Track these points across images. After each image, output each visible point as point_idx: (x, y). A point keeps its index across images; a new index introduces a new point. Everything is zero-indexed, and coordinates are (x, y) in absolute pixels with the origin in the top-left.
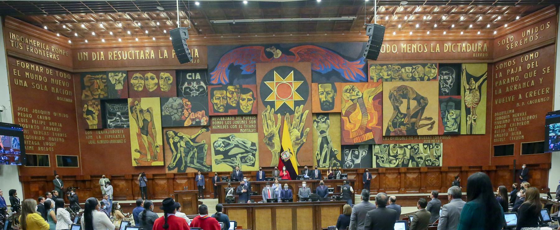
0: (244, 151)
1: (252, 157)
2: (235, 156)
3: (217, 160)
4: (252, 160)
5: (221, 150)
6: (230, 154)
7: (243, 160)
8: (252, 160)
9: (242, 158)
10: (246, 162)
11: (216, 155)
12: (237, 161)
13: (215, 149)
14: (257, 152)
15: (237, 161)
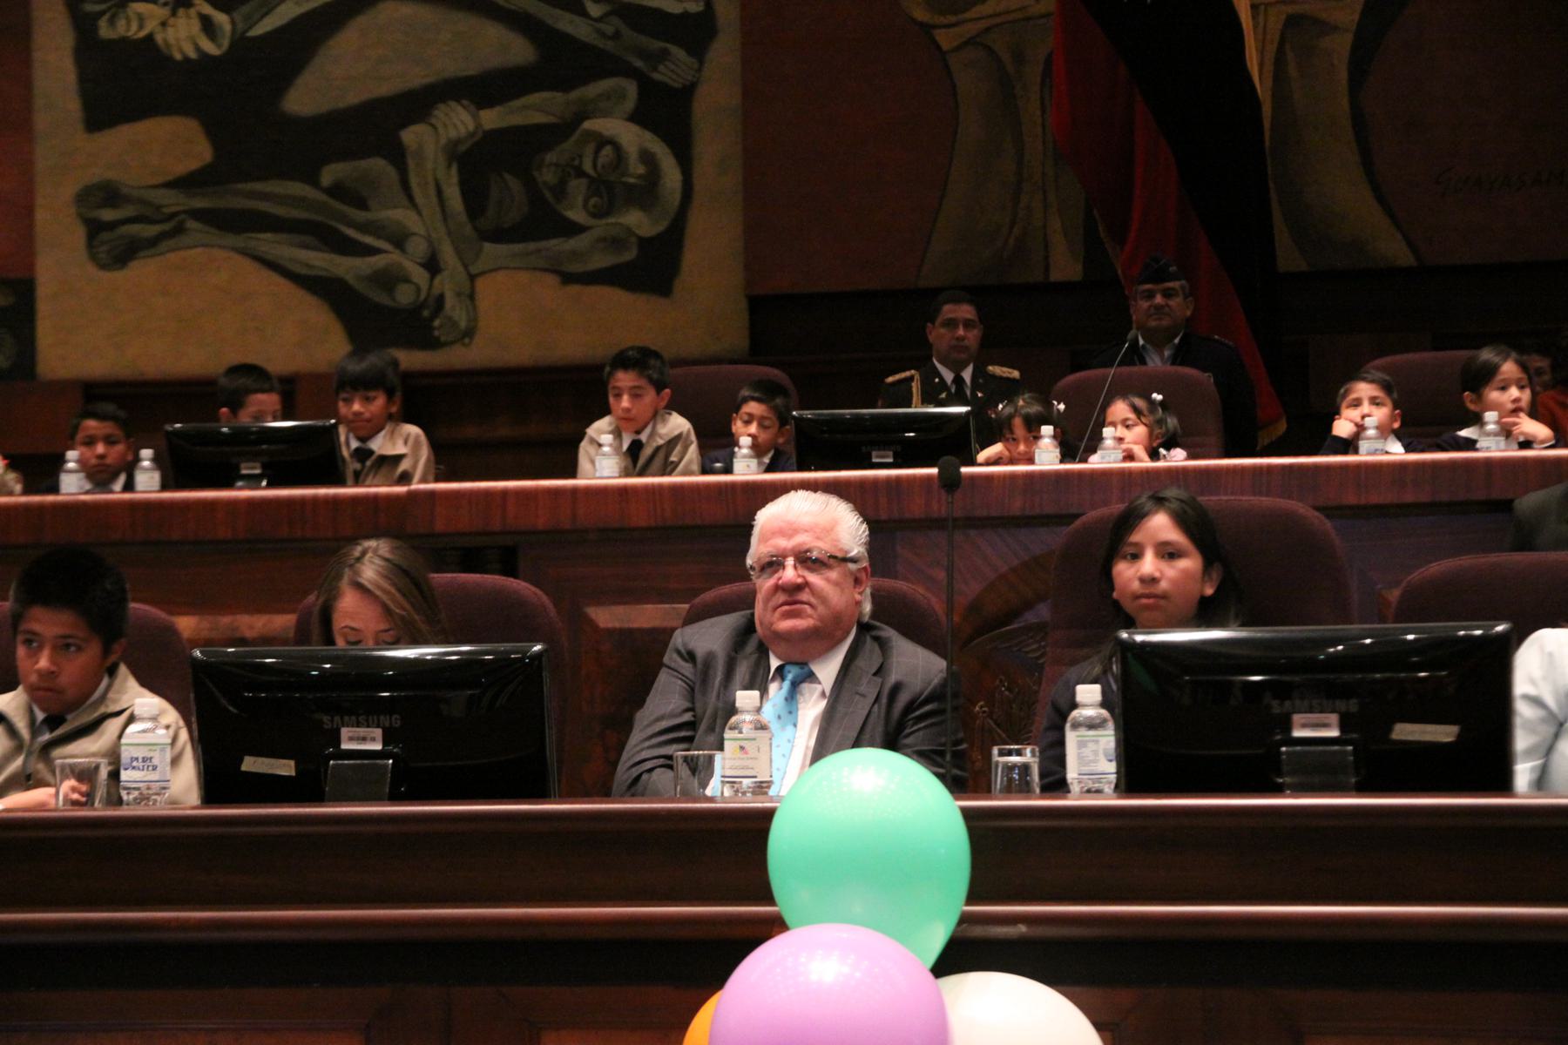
0: (517, 50)
1: (631, 137)
2: (377, 126)
3: (109, 194)
4: (646, 193)
5: (183, 37)
6: (306, 97)
7: (509, 194)
8: (646, 193)
9: (477, 163)
10: (542, 222)
11: (99, 116)
12: (415, 217)
13: (84, 26)
14: (724, 52)
15: (415, 217)
